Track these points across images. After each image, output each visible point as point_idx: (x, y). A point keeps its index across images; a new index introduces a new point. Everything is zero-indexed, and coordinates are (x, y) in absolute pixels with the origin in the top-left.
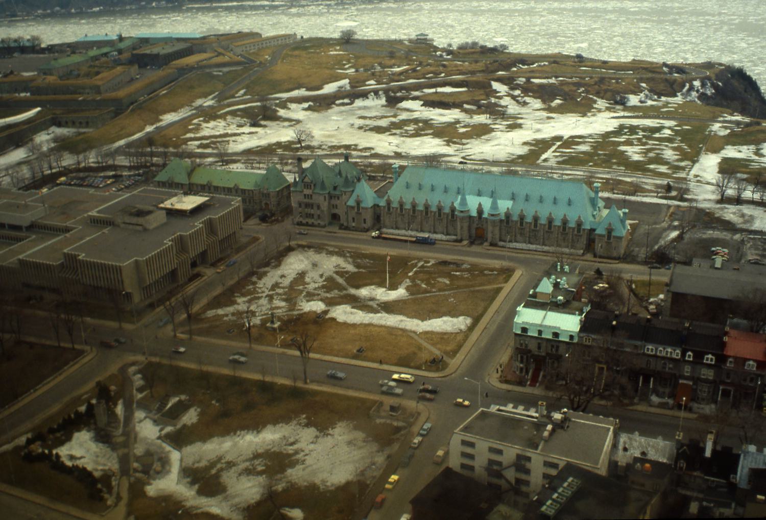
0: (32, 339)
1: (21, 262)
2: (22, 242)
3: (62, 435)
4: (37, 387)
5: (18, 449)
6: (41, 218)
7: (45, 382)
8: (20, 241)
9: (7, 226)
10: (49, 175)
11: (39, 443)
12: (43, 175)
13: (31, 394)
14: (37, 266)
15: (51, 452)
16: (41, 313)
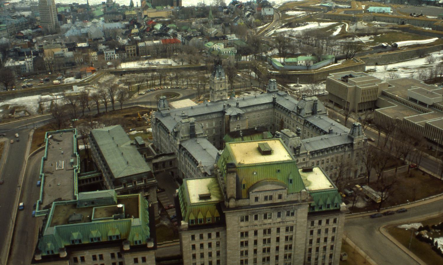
0: (423, 169)
1: (427, 125)
2: (426, 113)
3: (439, 232)
4: (427, 199)
5: (413, 230)
6: (438, 103)
7: (432, 197)
8: (424, 113)
9: (418, 102)
10: (439, 77)
11: (426, 231)
12: (436, 76)
13: (422, 201)
14: (435, 130)
15: (433, 240)
16: (432, 157)
